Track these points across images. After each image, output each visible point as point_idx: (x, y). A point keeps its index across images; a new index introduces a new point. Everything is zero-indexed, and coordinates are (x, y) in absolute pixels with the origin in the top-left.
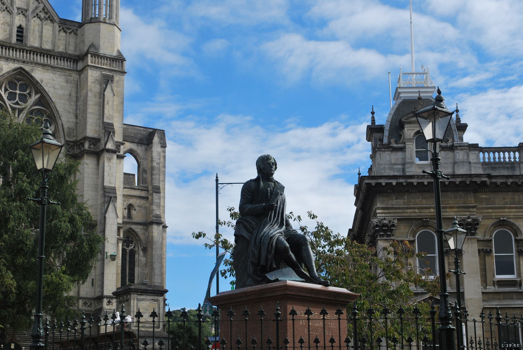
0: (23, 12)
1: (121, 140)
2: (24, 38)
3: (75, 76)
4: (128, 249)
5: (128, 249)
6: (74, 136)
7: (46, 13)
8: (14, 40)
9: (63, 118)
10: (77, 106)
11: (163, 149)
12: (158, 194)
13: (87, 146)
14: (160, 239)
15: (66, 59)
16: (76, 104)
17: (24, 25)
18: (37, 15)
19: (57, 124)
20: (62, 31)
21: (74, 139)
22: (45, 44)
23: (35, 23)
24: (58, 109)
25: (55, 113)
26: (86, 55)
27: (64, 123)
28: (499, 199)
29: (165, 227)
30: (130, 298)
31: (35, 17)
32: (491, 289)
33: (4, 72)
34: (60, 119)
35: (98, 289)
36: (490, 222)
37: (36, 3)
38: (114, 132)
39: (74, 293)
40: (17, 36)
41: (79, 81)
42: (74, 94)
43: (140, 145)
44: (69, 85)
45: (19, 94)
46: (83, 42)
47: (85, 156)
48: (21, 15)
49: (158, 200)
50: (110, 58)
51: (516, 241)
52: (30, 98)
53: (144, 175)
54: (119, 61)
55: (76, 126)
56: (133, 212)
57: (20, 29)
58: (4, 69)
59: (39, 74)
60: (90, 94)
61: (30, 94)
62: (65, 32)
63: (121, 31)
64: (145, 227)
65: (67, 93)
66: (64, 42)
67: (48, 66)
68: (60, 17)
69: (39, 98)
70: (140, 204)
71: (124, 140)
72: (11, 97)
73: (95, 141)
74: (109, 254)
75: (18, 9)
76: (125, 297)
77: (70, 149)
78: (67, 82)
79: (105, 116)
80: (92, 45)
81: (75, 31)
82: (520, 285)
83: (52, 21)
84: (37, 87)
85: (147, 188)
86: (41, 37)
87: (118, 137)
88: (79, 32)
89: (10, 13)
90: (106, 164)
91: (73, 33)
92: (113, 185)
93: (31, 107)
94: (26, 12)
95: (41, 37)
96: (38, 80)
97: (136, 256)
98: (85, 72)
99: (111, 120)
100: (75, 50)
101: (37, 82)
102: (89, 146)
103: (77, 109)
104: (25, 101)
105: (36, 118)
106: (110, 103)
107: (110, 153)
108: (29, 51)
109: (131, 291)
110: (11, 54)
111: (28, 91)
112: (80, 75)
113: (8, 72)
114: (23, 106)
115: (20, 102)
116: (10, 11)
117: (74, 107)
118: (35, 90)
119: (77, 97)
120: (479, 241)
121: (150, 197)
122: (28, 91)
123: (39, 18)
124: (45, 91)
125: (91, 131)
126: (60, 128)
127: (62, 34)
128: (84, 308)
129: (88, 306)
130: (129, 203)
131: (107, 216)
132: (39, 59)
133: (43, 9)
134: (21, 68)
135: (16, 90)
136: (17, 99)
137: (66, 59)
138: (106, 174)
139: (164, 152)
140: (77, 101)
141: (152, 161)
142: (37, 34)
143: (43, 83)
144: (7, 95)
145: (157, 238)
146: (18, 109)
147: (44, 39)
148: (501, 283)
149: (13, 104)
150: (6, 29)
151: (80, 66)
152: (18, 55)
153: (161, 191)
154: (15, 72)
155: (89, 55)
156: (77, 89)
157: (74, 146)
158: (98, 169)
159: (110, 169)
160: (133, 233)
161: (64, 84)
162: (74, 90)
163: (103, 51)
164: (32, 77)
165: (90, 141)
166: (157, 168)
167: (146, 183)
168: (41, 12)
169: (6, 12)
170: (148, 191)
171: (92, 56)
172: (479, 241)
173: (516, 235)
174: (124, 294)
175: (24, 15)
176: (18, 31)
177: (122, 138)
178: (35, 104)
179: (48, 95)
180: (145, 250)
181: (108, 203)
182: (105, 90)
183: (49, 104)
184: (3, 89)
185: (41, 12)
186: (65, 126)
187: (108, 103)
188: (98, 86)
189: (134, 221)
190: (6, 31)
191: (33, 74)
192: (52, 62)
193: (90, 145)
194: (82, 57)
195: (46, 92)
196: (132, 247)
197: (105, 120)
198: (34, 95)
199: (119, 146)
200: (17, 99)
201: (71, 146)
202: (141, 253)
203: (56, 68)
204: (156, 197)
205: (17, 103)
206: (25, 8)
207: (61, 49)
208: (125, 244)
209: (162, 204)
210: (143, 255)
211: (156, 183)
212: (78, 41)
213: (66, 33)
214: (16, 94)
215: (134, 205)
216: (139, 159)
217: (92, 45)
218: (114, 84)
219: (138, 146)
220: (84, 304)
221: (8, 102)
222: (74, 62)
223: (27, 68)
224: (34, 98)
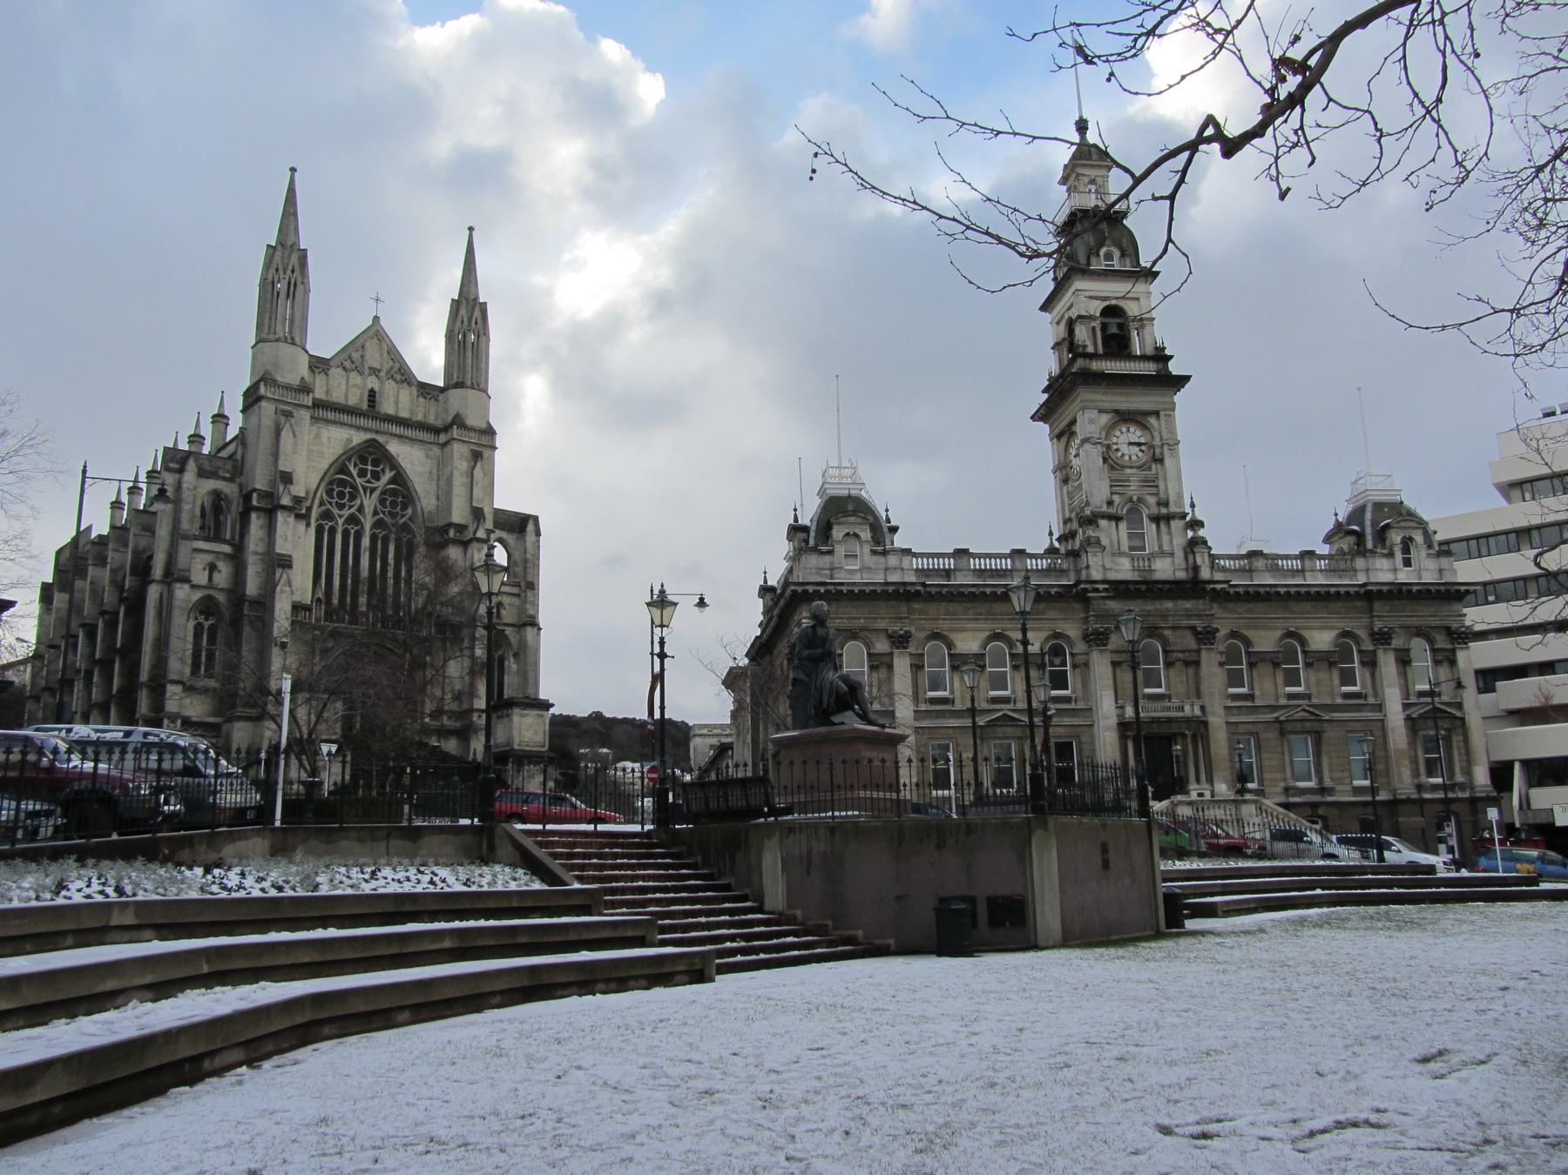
0: (375, 372)
1: (491, 527)
3: (436, 451)
7: (403, 375)
8: (365, 406)
10: (438, 485)
13: (452, 533)
17: (376, 388)
23: (389, 385)
25: (414, 494)
28: (932, 609)
30: (512, 714)
32: (923, 707)
33: (354, 444)
36: (923, 635)
37: (391, 363)
38: (484, 519)
40: (369, 401)
42: (435, 471)
44: (429, 461)
45: (372, 471)
46: (446, 410)
47: (450, 546)
48: (374, 377)
50: (479, 431)
51: (950, 655)
57: (372, 393)
59: (394, 447)
60: (456, 473)
61: (383, 471)
62: (425, 398)
65: (427, 470)
66: (423, 410)
67: (406, 437)
68: (419, 380)
71: (495, 527)
72: (362, 473)
73: (461, 528)
75: (370, 368)
78: (427, 457)
80: (457, 416)
82: (953, 703)
83: (409, 384)
84: (392, 463)
86: (397, 403)
87: (489, 524)
89: (361, 373)
91: (433, 400)
95: (397, 403)
98: (449, 446)
100: (436, 419)
101: (393, 457)
104: (378, 479)
106: (480, 485)
110: (362, 422)
113: (359, 445)
119: (438, 476)
120: (911, 654)
125: (459, 515)
126: (420, 512)
127: (422, 400)
132: (394, 429)
133: (399, 370)
140: (438, 480)
141: (525, 552)
142: (392, 399)
147: (400, 406)
148: (933, 701)
151: (443, 438)
152: (370, 424)
155: (455, 427)
161: (424, 460)
163: (469, 422)
164: (387, 450)
172: (911, 654)
173: (949, 648)
178: (390, 482)
182: (473, 468)
188: (465, 464)
192: (409, 433)
194: (447, 428)
197: (475, 504)
203: (416, 440)
205: (368, 481)
206: (378, 367)
207: (420, 417)
212: (440, 409)
214: (367, 470)
217: (457, 416)
218: (484, 461)
221: (359, 480)
223: (381, 439)
224: (388, 475)
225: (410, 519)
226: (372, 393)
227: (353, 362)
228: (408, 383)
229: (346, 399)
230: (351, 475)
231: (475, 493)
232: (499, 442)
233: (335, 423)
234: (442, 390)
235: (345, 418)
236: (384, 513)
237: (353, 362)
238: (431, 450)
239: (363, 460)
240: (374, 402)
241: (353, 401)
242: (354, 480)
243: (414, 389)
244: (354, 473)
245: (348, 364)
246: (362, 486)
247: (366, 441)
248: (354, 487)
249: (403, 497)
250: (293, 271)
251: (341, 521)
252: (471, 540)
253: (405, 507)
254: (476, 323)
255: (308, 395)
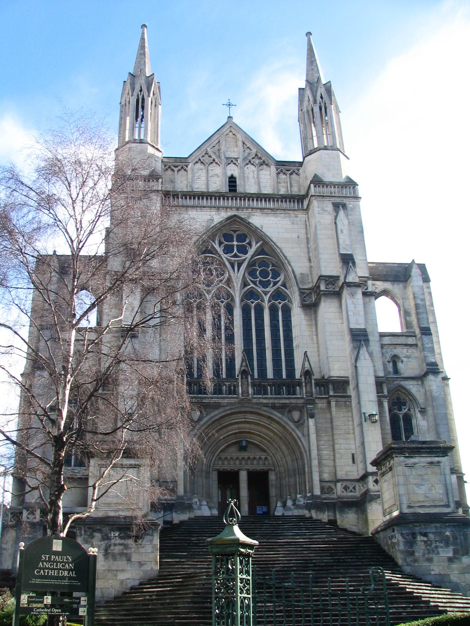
2: (237, 187)
4: (401, 412)
5: (401, 414)
6: (309, 283)
7: (260, 158)
8: (225, 189)
9: (292, 264)
10: (308, 248)
11: (425, 285)
12: (428, 337)
14: (440, 394)
15: (288, 200)
16: (308, 246)
17: (236, 174)
18: (250, 162)
19: (287, 272)
20: (281, 174)
21: (310, 286)
22: (262, 189)
24: (286, 254)
26: (309, 187)
27: (295, 269)
29: (445, 379)
31: (248, 164)
34: (290, 265)
35: (361, 466)
39: (329, 474)
40: (230, 186)
41: (307, 220)
42: (303, 236)
43: (396, 283)
44: (295, 226)
45: (237, 246)
46: (306, 177)
49: (430, 344)
52: (251, 248)
53: (408, 318)
54: (350, 188)
55: (311, 271)
56: (400, 366)
57: (232, 181)
58: (215, 220)
61: (250, 244)
63: (348, 158)
64: (420, 382)
65: (295, 236)
69: (261, 246)
70: (408, 354)
72: (228, 250)
74: (367, 415)
75: (227, 158)
76: (388, 463)
77: (307, 298)
78: (293, 224)
79: (341, 247)
81: (296, 171)
85: (414, 333)
88: (301, 171)
90: (349, 302)
92: (363, 327)
93: (252, 257)
94: (237, 160)
96: (258, 226)
97: (414, 421)
98: (311, 207)
99: (348, 251)
102: (326, 287)
103: (309, 252)
104: (246, 253)
105: (260, 269)
107: (353, 288)
108: (242, 197)
109: (392, 453)
111: (247, 241)
112: (308, 213)
114: (243, 258)
115: (239, 254)
116: (218, 162)
117: (306, 250)
118: (255, 239)
121: (419, 344)
122: (247, 241)
123: (252, 164)
124: (267, 236)
127: (282, 176)
128: (345, 494)
129: (351, 491)
130: (393, 354)
131: (358, 365)
133: (256, 155)
134: (235, 216)
135: (233, 241)
136: (235, 251)
137: (288, 200)
138: (350, 313)
139: (429, 287)
143: (263, 228)
144: (223, 248)
145: (437, 392)
146: (238, 261)
149: (232, 257)
150: (216, 181)
153: (432, 331)
154: (229, 221)
155: (312, 186)
156: (306, 229)
157: (311, 293)
158: (342, 312)
159: (355, 307)
160: (404, 391)
162: (303, 231)
163: (328, 177)
164: (249, 223)
165: (326, 281)
166: (423, 305)
167: (412, 327)
168: (253, 158)
169: (214, 164)
170: (415, 336)
171: (315, 186)
174: (385, 459)
175: (234, 164)
176: (230, 182)
177: (368, 272)
178: (257, 253)
179: (272, 241)
180: (423, 411)
181: (357, 349)
182: (336, 218)
183: (274, 251)
184: (217, 242)
185: (253, 158)
186: (297, 273)
187: (342, 232)
189: (402, 376)
190: (216, 183)
191: (250, 221)
193: (327, 284)
195: (269, 237)
196: (406, 410)
197: (342, 252)
198: (254, 244)
199: (366, 282)
200: (235, 251)
201: (308, 295)
202: (419, 415)
204: (426, 341)
205: (235, 256)
207: (282, 191)
208: (396, 407)
209: (436, 351)
210: (422, 418)
211: (423, 324)
213: (286, 175)
214: (233, 246)
215: (401, 356)
216: (397, 300)
219: (393, 285)
220: (344, 488)
221: (224, 256)
222: (298, 202)
223: (242, 214)
224: (255, 247)
225: (284, 285)
226: (232, 181)
227: (210, 156)
228: (267, 165)
229: (208, 187)
230: (216, 253)
231: (341, 241)
232: (361, 191)
233: (193, 207)
234: (301, 164)
235: (205, 202)
236: (254, 283)
237: (210, 156)
238: (297, 217)
239: (228, 237)
240: (235, 186)
241: (213, 188)
242: (220, 256)
243: (273, 168)
244: (220, 250)
245: (206, 159)
246: (229, 261)
247: (229, 218)
248: (222, 263)
249: (273, 265)
250: (141, 91)
251: (208, 297)
252: (342, 288)
253: (276, 275)
254: (322, 98)
255: (157, 181)
